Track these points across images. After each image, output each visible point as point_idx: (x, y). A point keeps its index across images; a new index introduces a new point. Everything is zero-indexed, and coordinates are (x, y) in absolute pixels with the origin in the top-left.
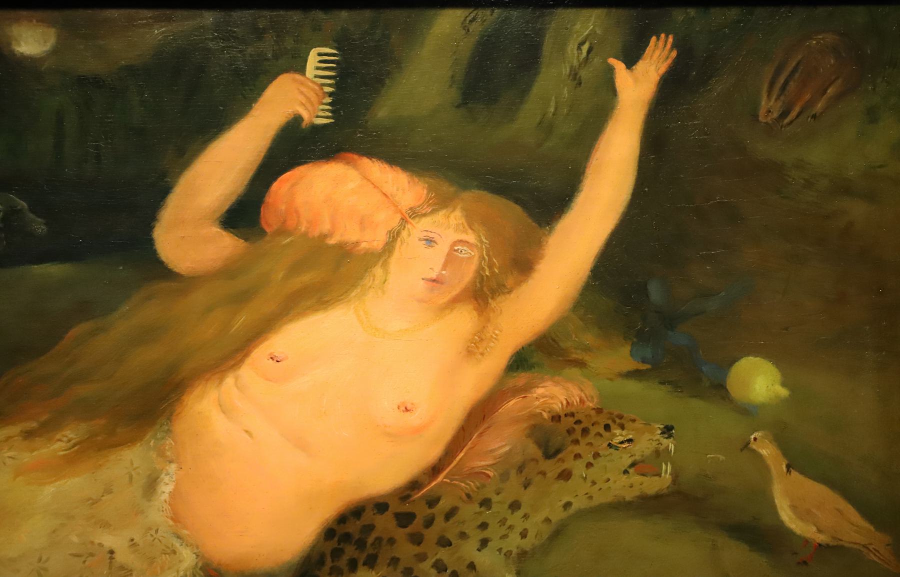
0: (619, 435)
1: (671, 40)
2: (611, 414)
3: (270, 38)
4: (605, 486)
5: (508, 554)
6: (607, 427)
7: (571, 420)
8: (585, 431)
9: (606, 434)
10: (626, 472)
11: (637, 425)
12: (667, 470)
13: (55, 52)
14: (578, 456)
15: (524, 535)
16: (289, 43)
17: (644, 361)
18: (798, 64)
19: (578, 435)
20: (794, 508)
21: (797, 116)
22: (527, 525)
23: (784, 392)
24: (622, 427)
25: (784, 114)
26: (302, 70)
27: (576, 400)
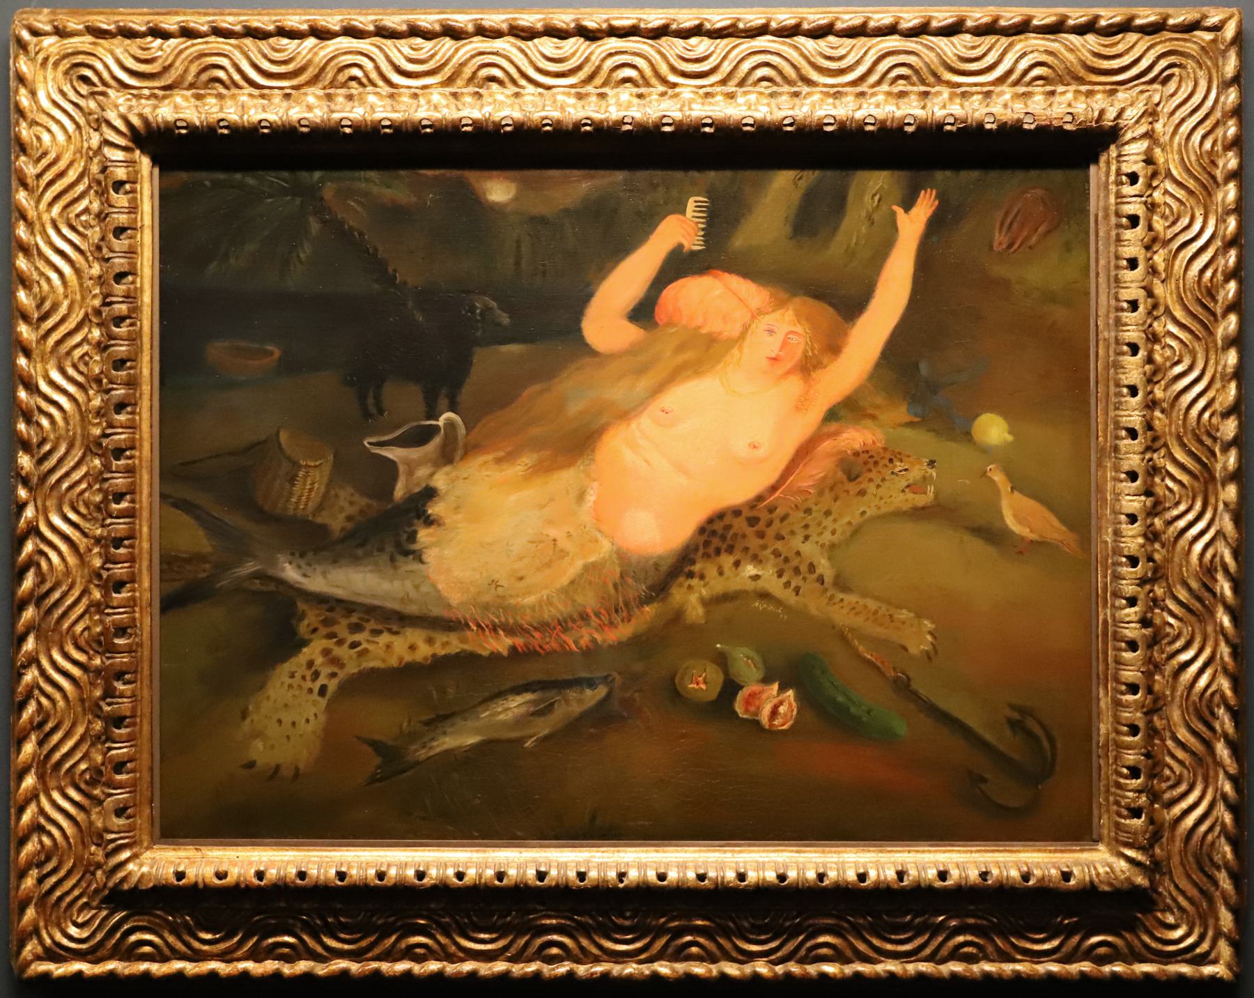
0: (899, 466)
1: (934, 192)
2: (893, 451)
3: (661, 190)
4: (889, 500)
5: (823, 546)
6: (891, 461)
7: (866, 456)
8: (876, 463)
9: (891, 465)
10: (903, 491)
11: (911, 459)
12: (931, 490)
13: (516, 199)
14: (871, 480)
15: (833, 533)
16: (675, 193)
17: (916, 415)
18: (1018, 212)
19: (871, 465)
20: (1015, 516)
21: (1019, 247)
22: (836, 526)
23: (1010, 438)
24: (901, 461)
25: (1010, 246)
26: (683, 212)
27: (870, 441)
